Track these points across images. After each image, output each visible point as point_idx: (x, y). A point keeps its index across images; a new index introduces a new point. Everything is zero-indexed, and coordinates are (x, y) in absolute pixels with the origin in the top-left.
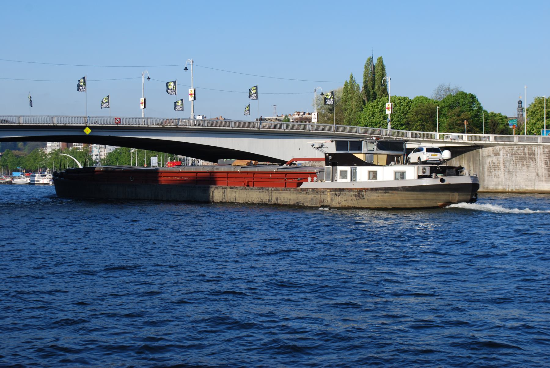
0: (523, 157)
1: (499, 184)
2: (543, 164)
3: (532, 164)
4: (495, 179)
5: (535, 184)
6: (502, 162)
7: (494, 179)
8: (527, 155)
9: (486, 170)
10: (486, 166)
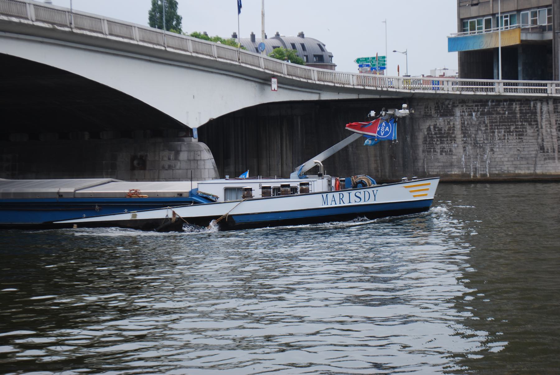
0: (508, 118)
1: (452, 165)
2: (554, 130)
3: (530, 131)
4: (443, 158)
5: (535, 164)
7: (439, 156)
8: (518, 115)
9: (420, 141)
10: (420, 137)
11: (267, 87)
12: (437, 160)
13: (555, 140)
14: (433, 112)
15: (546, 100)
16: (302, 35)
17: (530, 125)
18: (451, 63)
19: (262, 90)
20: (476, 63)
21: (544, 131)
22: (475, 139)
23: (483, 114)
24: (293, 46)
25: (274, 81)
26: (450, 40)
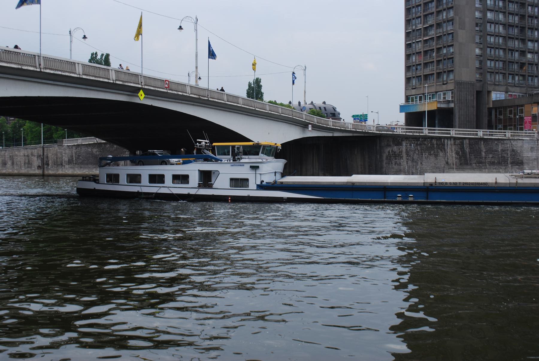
2: (454, 154)
3: (441, 154)
6: (404, 151)
7: (394, 166)
9: (384, 158)
11: (306, 129)
12: (393, 168)
13: (454, 159)
14: (391, 143)
15: (450, 138)
16: (324, 103)
17: (441, 151)
18: (401, 118)
19: (304, 131)
20: (414, 119)
21: (448, 154)
22: (413, 158)
23: (417, 145)
24: (320, 108)
25: (310, 126)
26: (401, 106)
